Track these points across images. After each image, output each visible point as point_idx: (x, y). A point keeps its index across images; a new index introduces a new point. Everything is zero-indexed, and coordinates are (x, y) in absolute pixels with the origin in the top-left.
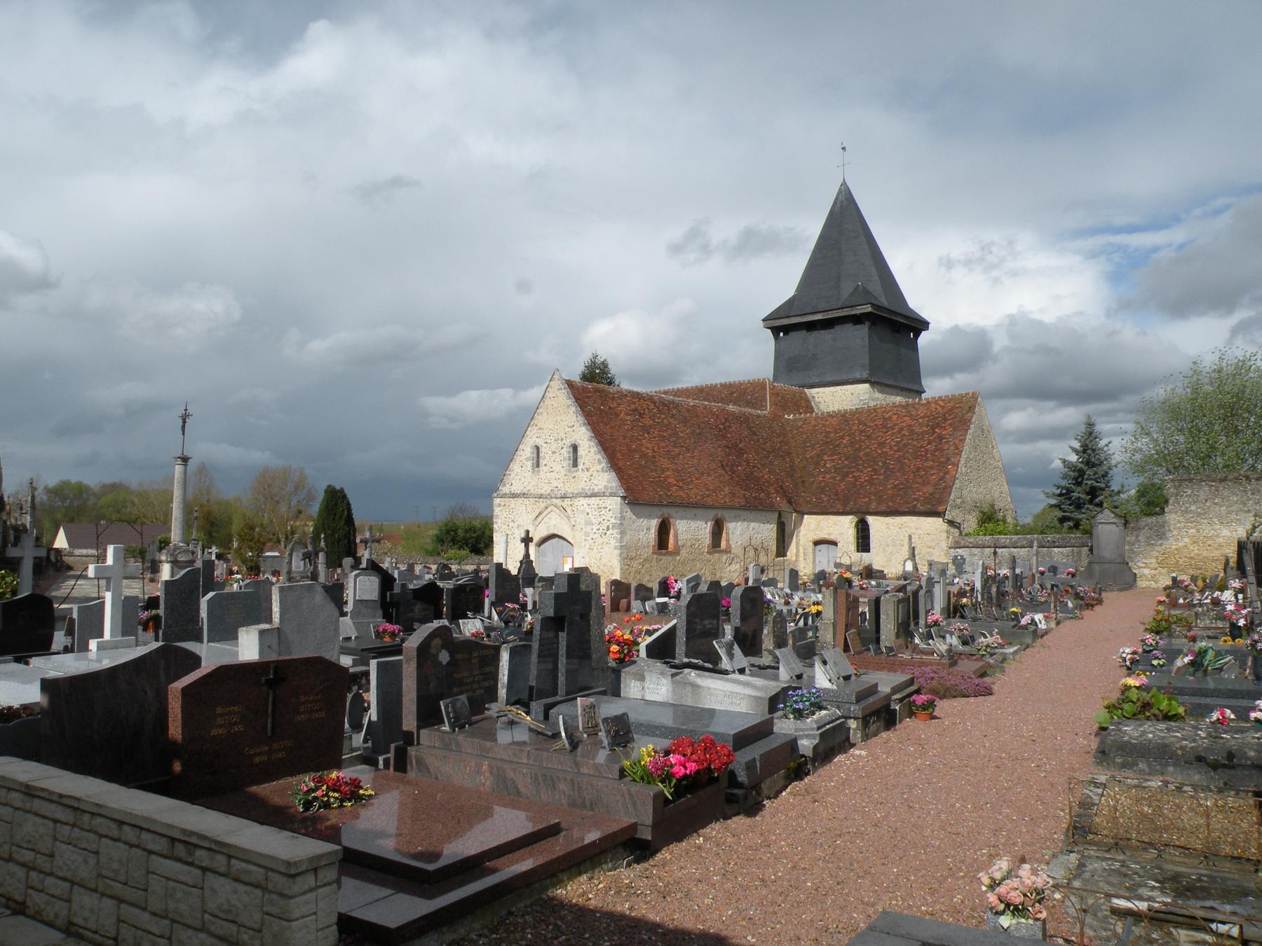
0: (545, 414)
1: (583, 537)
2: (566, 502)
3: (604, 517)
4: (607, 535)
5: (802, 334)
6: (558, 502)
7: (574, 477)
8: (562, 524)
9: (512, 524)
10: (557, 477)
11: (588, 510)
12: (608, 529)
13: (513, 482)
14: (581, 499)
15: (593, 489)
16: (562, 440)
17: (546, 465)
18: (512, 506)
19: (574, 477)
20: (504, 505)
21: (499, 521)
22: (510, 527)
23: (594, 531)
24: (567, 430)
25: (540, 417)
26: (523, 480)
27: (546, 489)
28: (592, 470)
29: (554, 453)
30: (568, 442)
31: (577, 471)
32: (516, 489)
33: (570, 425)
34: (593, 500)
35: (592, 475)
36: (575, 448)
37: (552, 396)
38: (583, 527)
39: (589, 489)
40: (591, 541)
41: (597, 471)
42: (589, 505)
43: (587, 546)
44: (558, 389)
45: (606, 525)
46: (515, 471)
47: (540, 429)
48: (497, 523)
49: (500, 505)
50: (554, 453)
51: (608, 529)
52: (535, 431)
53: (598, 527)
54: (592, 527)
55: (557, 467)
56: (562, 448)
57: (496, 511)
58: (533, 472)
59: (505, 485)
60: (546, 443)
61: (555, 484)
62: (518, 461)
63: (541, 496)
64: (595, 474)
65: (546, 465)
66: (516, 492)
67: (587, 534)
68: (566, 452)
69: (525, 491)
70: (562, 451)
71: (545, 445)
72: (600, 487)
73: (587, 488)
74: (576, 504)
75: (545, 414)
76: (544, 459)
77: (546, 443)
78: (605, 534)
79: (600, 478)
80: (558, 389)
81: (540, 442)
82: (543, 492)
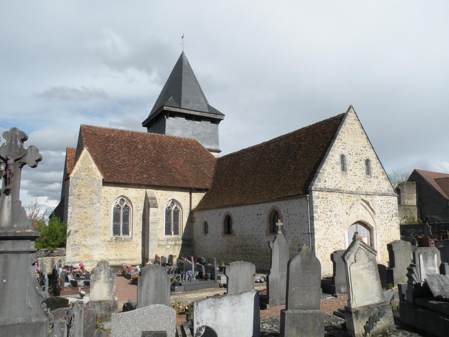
0: (347, 133)
1: (380, 222)
2: (368, 199)
3: (390, 209)
4: (393, 221)
5: (183, 120)
6: (364, 197)
7: (370, 182)
8: (366, 213)
9: (329, 213)
10: (359, 180)
11: (381, 204)
12: (393, 217)
13: (327, 179)
14: (377, 196)
15: (382, 191)
16: (360, 154)
17: (351, 170)
18: (330, 198)
19: (370, 182)
20: (323, 198)
21: (319, 211)
22: (329, 216)
23: (386, 218)
24: (362, 149)
25: (343, 135)
26: (335, 179)
27: (353, 188)
28: (379, 178)
29: (356, 162)
30: (364, 157)
31: (371, 178)
32: (330, 184)
33: (364, 146)
34: (383, 198)
35: (380, 182)
36: (367, 162)
37: (351, 122)
38: (379, 215)
39: (379, 190)
40: (385, 225)
41: (383, 179)
42: (382, 201)
43: (383, 229)
44: (355, 120)
45: (391, 214)
46: (328, 171)
47: (344, 143)
48: (317, 212)
49: (318, 197)
50: (356, 162)
51: (393, 217)
52: (340, 144)
53: (387, 215)
54: (384, 215)
55: (359, 173)
56: (361, 160)
57: (315, 202)
58: (342, 174)
59: (319, 181)
60: (350, 154)
61: (359, 185)
62: (329, 164)
63: (352, 193)
64: (381, 181)
65: (351, 170)
66: (330, 187)
67: (382, 220)
68: (363, 163)
69: (337, 187)
70: (361, 162)
71: (349, 156)
72: (385, 190)
73: (378, 189)
74: (374, 200)
75: (347, 133)
76: (350, 165)
77: (350, 154)
78: (392, 220)
79: (384, 184)
80: (355, 120)
81: (345, 153)
82: (350, 189)
